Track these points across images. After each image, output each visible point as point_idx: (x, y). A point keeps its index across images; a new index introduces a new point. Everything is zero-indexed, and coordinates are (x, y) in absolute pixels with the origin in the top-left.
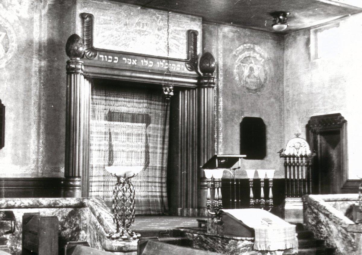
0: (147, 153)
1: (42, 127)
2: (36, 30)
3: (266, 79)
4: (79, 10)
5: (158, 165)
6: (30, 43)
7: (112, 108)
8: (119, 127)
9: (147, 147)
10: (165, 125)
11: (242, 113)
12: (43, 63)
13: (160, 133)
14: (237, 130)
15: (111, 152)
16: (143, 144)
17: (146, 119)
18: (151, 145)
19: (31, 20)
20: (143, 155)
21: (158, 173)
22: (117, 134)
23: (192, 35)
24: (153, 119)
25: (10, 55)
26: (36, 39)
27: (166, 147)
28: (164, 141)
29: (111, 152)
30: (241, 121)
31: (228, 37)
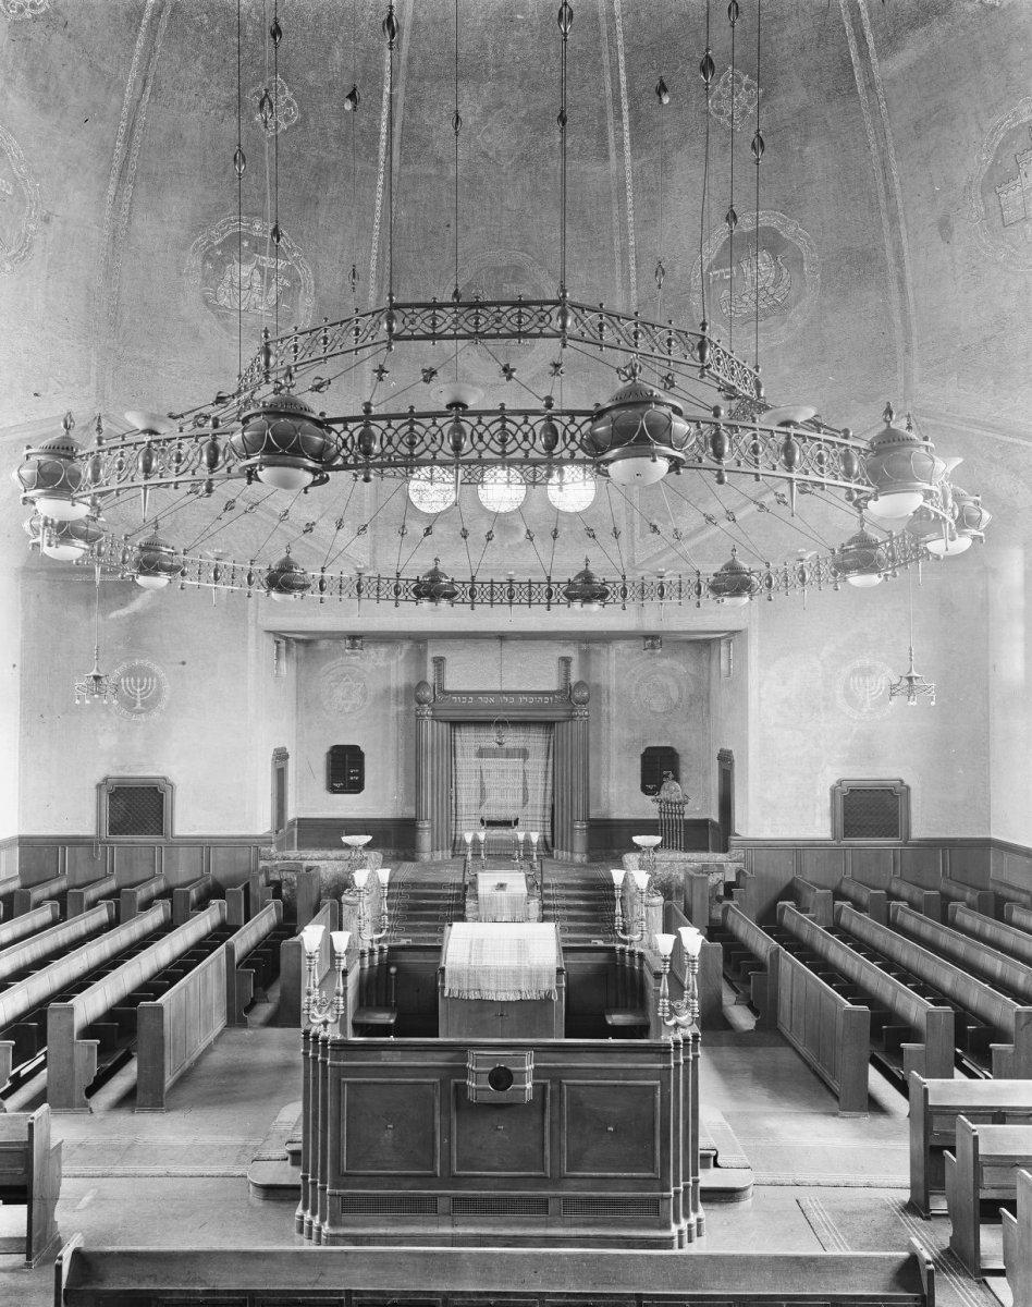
0: (525, 790)
1: (401, 769)
2: (393, 676)
3: (680, 699)
4: (431, 654)
5: (539, 802)
6: (387, 691)
7: (483, 745)
8: (490, 763)
9: (525, 783)
10: (548, 758)
11: (645, 741)
12: (401, 708)
13: (541, 768)
14: (638, 762)
15: (483, 789)
16: (521, 781)
17: (524, 754)
18: (529, 781)
19: (388, 668)
20: (521, 792)
21: (539, 811)
22: (488, 771)
23: (566, 661)
24: (531, 753)
25: (368, 703)
26: (393, 686)
27: (550, 782)
28: (546, 777)
29: (483, 789)
30: (642, 751)
31: (623, 655)
